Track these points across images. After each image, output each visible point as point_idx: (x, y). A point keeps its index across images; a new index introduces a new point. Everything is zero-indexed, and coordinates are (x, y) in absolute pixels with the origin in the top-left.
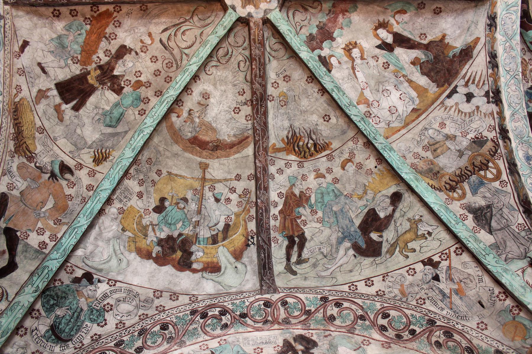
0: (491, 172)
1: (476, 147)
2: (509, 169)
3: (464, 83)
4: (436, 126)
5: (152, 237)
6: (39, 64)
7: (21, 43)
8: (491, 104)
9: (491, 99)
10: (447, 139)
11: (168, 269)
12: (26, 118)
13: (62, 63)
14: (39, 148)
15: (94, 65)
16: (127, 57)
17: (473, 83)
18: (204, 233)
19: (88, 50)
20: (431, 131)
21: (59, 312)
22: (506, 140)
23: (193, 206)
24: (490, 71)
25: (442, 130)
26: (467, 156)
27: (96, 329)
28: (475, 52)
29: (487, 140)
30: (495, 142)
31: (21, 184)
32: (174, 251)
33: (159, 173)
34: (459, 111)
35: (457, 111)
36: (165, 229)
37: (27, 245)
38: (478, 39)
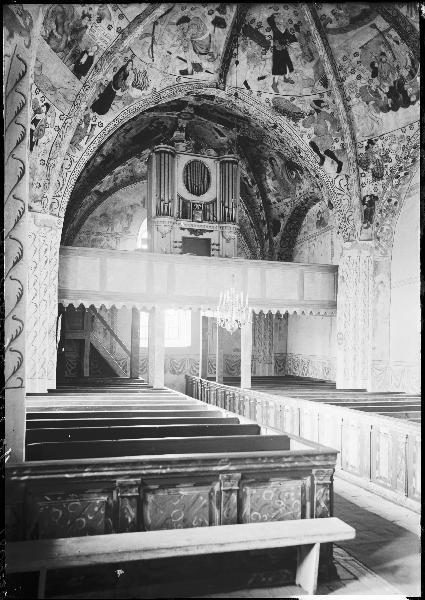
5: (384, 96)
6: (259, 79)
7: (244, 86)
11: (401, 110)
12: (283, 105)
13: (263, 63)
14: (300, 106)
15: (272, 41)
16: (276, 20)
18: (405, 73)
19: (263, 43)
21: (371, 166)
23: (389, 55)
27: (389, 165)
31: (311, 130)
32: (398, 97)
33: (356, 54)
36: (386, 84)
37: (337, 151)
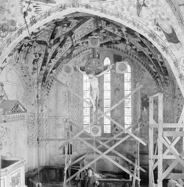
0: (3, 34)
1: (10, 23)
2: (8, 39)
3: (34, 5)
4: (11, 4)
8: (29, 20)
9: (32, 19)
10: (7, 11)
17: (36, 9)
20: (7, 4)
22: (18, 34)
24: (43, 14)
25: (10, 7)
26: (5, 22)
28: (49, 4)
29: (15, 26)
30: (15, 29)
34: (22, 9)
35: (21, 8)
38: (55, 3)
